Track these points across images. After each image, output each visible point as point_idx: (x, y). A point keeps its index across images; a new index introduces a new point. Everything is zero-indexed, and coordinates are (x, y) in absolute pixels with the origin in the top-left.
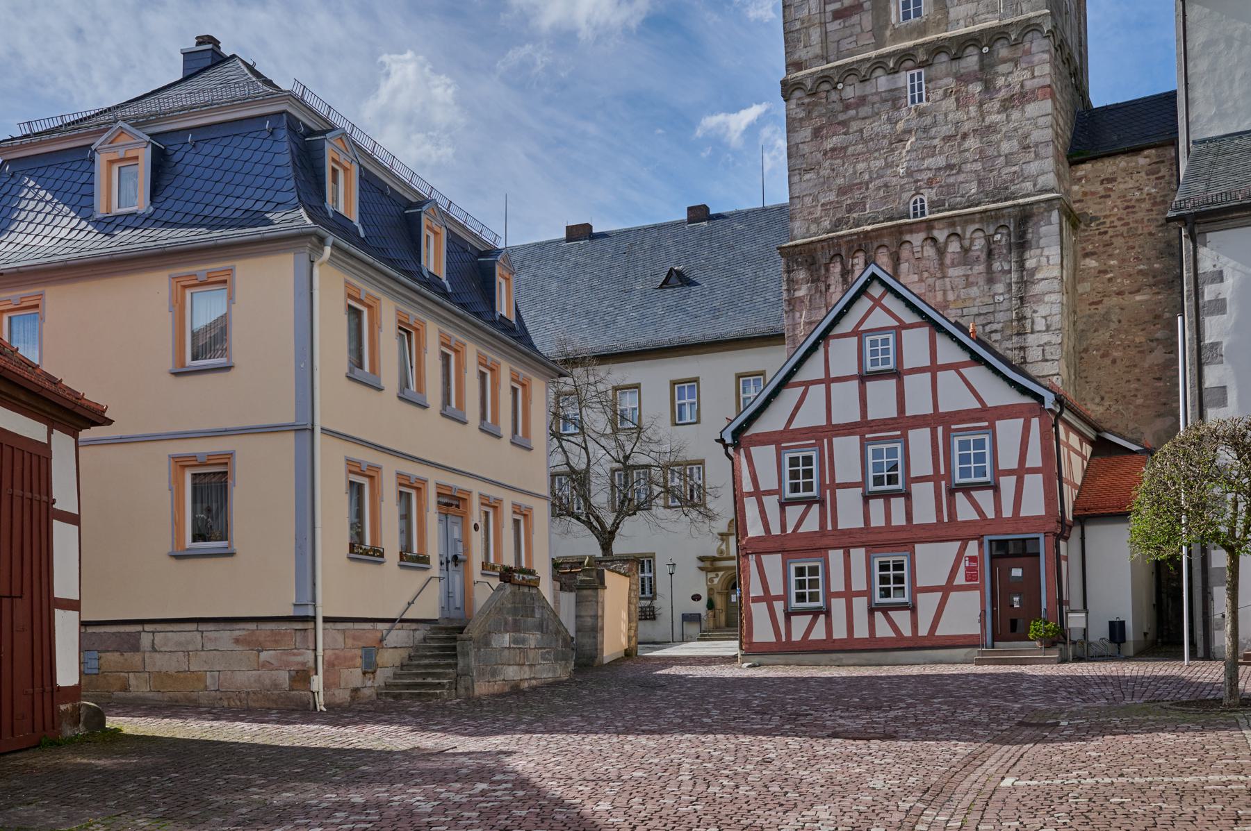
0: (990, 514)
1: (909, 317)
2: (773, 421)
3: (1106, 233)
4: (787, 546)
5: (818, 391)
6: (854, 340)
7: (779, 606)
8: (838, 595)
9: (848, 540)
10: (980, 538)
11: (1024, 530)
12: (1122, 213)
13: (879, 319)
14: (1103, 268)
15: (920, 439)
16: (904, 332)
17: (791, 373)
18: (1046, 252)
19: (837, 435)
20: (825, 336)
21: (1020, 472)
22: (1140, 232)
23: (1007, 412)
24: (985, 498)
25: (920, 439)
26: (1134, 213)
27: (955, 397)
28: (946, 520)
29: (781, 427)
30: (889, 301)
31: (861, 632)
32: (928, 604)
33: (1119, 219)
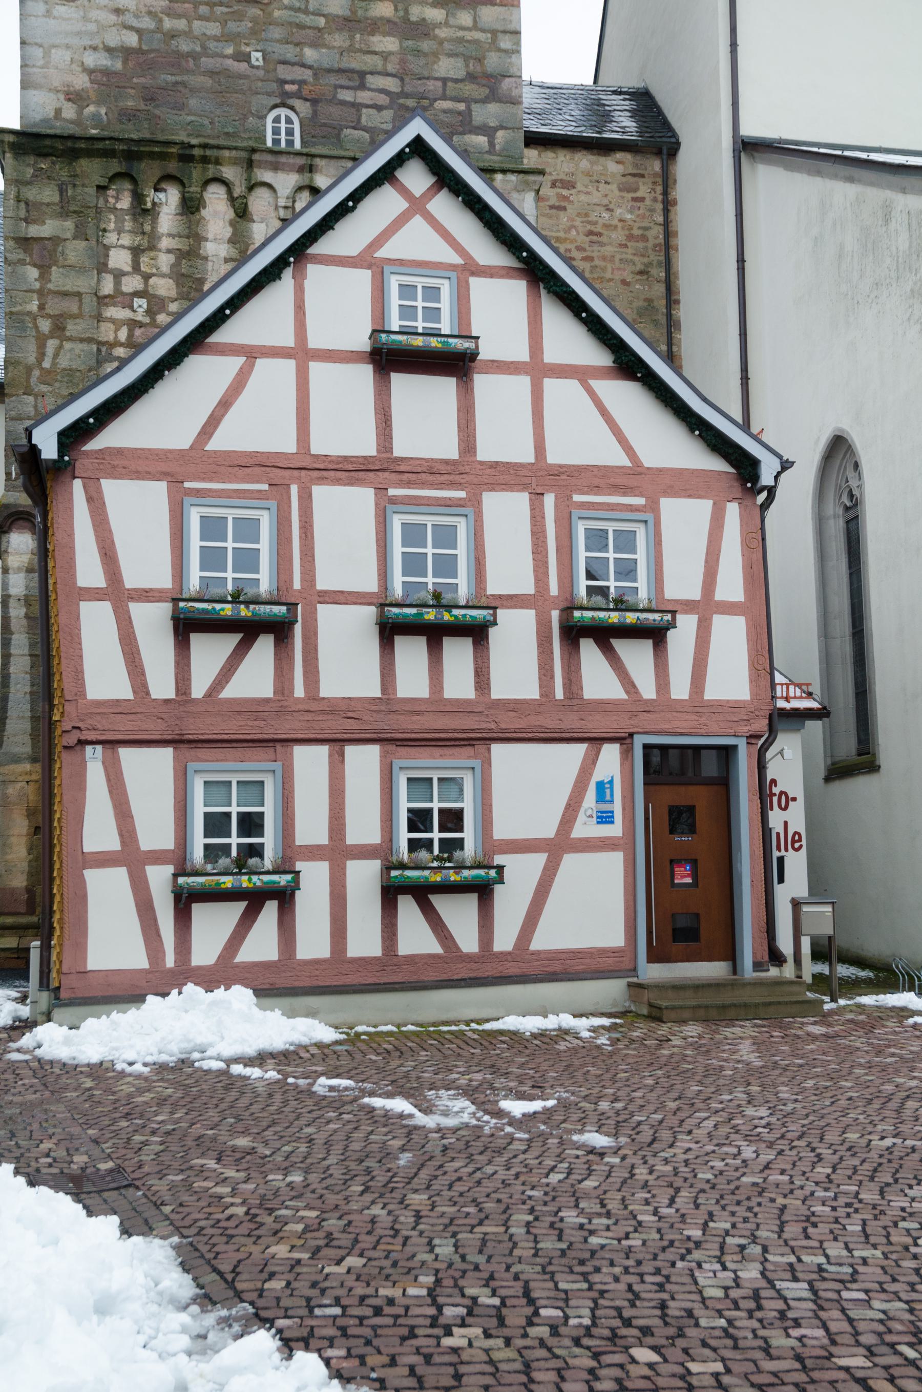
0: (648, 690)
1: (486, 251)
5: (274, 378)
6: (364, 277)
7: (159, 878)
8: (313, 853)
9: (341, 728)
10: (625, 740)
11: (715, 729)
12: (583, 240)
13: (416, 242)
15: (506, 516)
16: (474, 281)
19: (321, 481)
20: (298, 252)
22: (608, 275)
23: (682, 484)
24: (637, 656)
25: (506, 516)
26: (601, 244)
29: (182, 440)
30: (444, 206)
31: (364, 941)
33: (579, 248)
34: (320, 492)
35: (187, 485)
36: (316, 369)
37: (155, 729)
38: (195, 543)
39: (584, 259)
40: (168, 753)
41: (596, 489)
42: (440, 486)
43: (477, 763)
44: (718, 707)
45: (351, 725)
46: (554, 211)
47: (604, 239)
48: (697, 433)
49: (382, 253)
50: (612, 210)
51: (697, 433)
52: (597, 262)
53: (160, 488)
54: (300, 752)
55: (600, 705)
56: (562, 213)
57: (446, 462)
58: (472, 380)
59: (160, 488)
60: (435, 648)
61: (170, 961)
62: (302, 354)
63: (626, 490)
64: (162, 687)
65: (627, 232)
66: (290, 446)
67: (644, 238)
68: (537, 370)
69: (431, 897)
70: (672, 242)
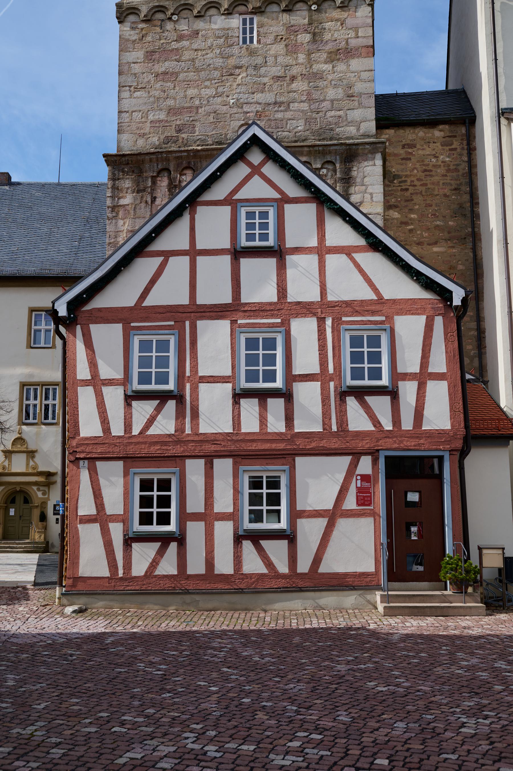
1: (293, 190)
2: (122, 295)
3: (407, 190)
4: (132, 453)
5: (179, 266)
6: (228, 209)
8: (196, 517)
9: (211, 448)
10: (374, 454)
12: (421, 175)
14: (405, 220)
16: (287, 207)
17: (149, 239)
18: (370, 190)
19: (202, 318)
21: (423, 377)
22: (436, 193)
23: (408, 307)
25: (304, 331)
26: (431, 176)
27: (346, 283)
28: (334, 428)
29: (131, 302)
30: (270, 169)
32: (310, 531)
33: (418, 180)
34: (200, 324)
35: (132, 324)
36: (200, 259)
37: (117, 451)
38: (136, 354)
39: (421, 185)
40: (121, 463)
41: (357, 313)
42: (267, 317)
43: (286, 467)
44: (431, 434)
45: (218, 448)
46: (404, 161)
47: (433, 173)
48: (415, 278)
49: (236, 197)
50: (438, 157)
51: (415, 278)
52: (429, 186)
53: (118, 328)
54: (190, 463)
55: (359, 435)
56: (408, 162)
57: (271, 304)
58: (285, 259)
59: (120, 326)
60: (263, 406)
61: (121, 573)
62: (193, 253)
63: (374, 313)
64: (117, 429)
65: (446, 168)
66: (186, 301)
67: (456, 170)
68: (322, 251)
69: (261, 542)
70: (473, 170)
